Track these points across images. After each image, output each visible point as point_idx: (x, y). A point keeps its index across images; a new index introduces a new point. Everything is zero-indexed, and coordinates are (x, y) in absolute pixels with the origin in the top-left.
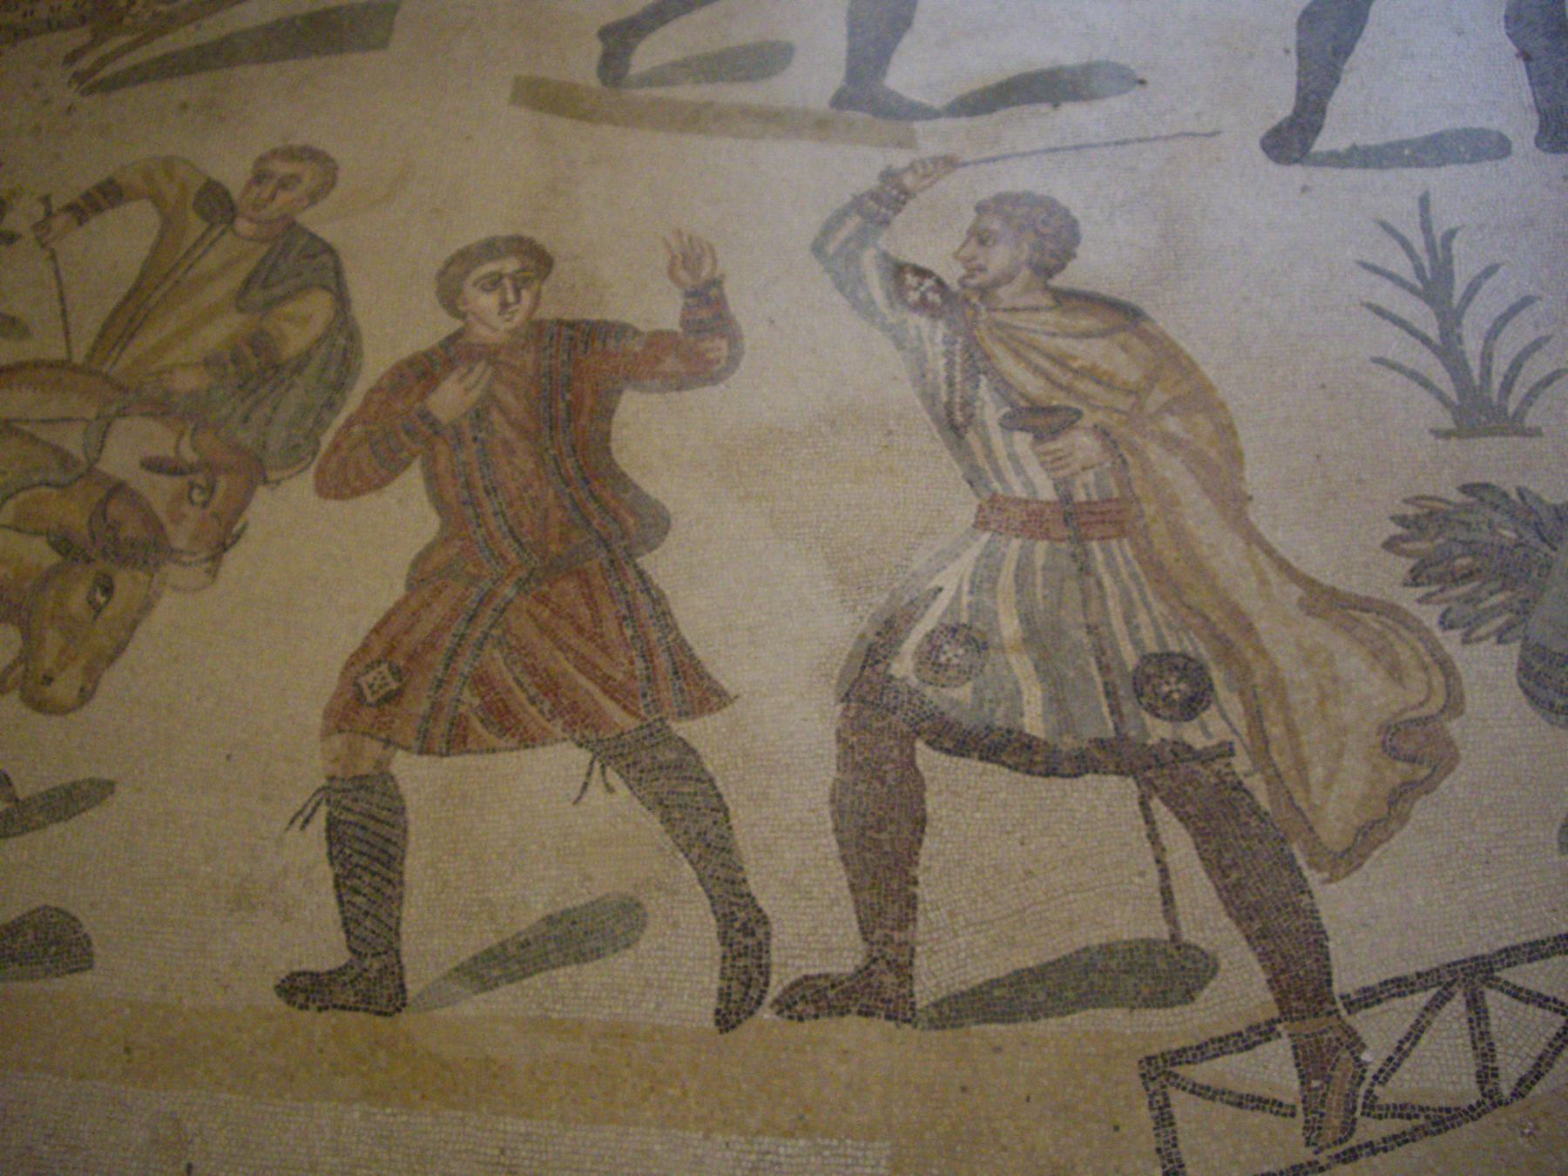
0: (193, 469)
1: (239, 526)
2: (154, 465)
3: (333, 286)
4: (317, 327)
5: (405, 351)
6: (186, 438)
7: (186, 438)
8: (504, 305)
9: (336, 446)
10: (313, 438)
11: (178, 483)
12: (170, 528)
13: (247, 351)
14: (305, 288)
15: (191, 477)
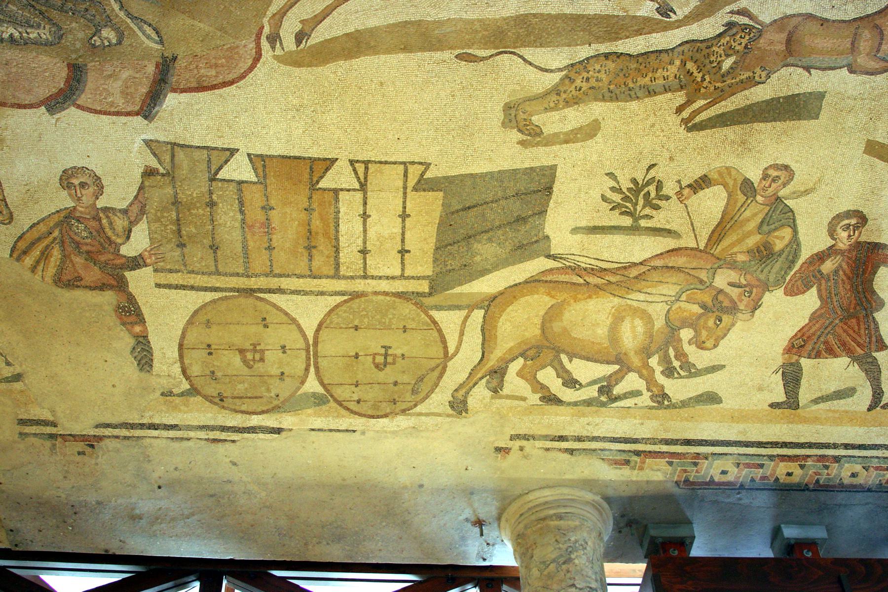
0: (745, 286)
1: (760, 303)
2: (731, 284)
3: (792, 226)
4: (786, 241)
5: (815, 251)
6: (743, 276)
7: (743, 276)
8: (849, 236)
9: (791, 280)
10: (784, 278)
11: (740, 290)
12: (738, 303)
13: (763, 249)
14: (782, 226)
15: (745, 288)
